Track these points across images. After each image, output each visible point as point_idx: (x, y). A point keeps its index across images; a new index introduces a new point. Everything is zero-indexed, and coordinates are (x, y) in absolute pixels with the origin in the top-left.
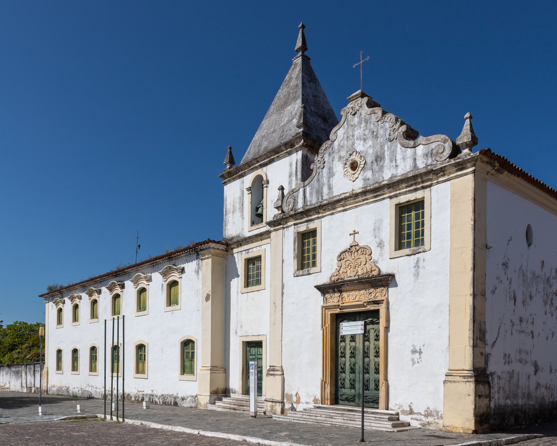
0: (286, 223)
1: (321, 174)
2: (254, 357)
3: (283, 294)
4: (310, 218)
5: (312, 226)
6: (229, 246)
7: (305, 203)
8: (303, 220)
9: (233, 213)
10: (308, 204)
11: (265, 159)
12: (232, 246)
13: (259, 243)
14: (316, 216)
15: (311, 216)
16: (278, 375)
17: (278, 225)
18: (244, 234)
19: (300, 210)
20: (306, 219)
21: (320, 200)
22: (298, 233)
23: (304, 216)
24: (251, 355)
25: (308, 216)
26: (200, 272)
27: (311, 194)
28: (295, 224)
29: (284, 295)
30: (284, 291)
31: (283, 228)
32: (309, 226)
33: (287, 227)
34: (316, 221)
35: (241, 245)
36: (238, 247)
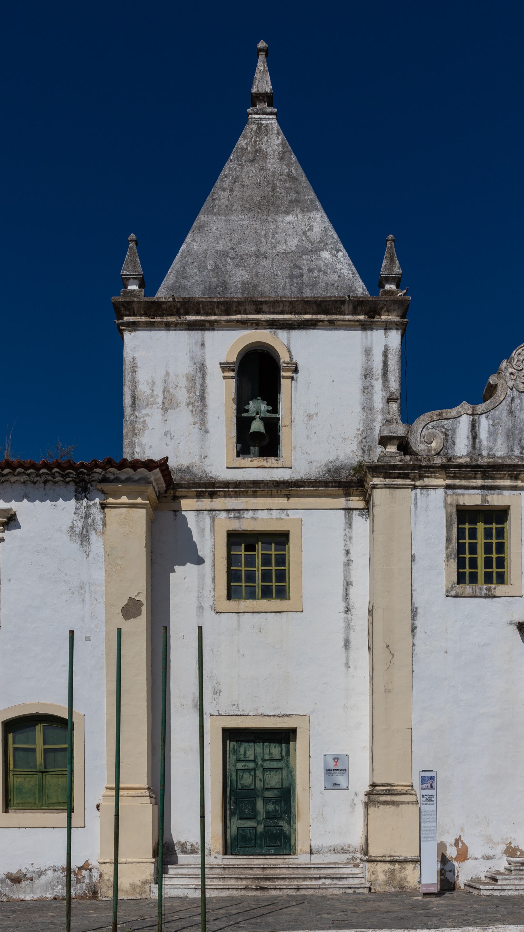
0: (421, 477)
1: (517, 401)
2: (252, 765)
3: (414, 628)
4: (489, 482)
5: (496, 500)
6: (168, 488)
7: (474, 448)
8: (473, 483)
9: (165, 410)
10: (485, 453)
11: (282, 313)
12: (180, 491)
13: (281, 502)
14: (508, 483)
15: (494, 478)
16: (408, 803)
17: (398, 478)
18: (208, 470)
19: (461, 461)
20: (479, 482)
21: (517, 452)
22: (458, 506)
23: (479, 475)
24: (238, 761)
25: (484, 477)
26: (93, 537)
27: (492, 434)
28: (448, 487)
29: (418, 631)
30: (418, 622)
31: (415, 487)
32: (489, 498)
33: (423, 487)
34: (506, 492)
35: (212, 495)
36: (199, 496)
